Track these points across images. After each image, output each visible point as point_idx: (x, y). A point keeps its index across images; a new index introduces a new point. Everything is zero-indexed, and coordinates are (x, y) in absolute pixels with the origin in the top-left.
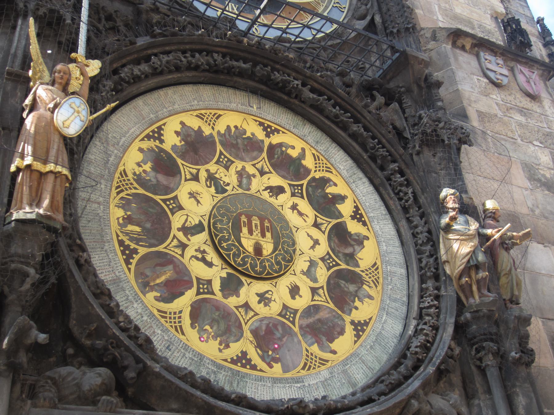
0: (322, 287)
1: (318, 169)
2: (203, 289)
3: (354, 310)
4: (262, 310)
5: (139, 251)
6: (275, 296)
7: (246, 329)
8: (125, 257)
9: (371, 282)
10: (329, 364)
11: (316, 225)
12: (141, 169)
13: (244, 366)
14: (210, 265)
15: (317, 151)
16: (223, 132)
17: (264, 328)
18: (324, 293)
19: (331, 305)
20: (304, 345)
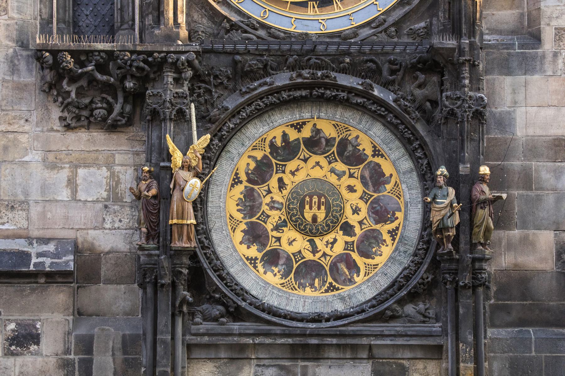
0: (349, 169)
4: (364, 213)
6: (354, 202)
7: (374, 227)
9: (347, 133)
10: (398, 181)
11: (305, 160)
12: (278, 274)
13: (396, 234)
14: (335, 240)
16: (242, 215)
17: (374, 216)
19: (361, 166)
20: (385, 193)
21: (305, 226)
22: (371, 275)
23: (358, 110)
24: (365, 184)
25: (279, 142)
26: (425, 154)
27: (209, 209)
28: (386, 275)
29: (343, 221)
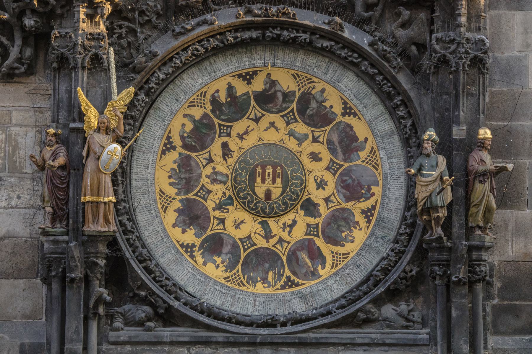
0: (313, 132)
1: (203, 105)
2: (314, 231)
3: (332, 110)
5: (288, 275)
6: (319, 174)
7: (344, 205)
8: (294, 286)
10: (375, 147)
11: (257, 120)
12: (221, 265)
13: (372, 215)
14: (295, 222)
15: (186, 102)
16: (176, 191)
17: (344, 191)
18: (317, 132)
19: (328, 128)
20: (358, 162)
21: (255, 204)
22: (339, 267)
23: (324, 56)
24: (332, 150)
25: (223, 97)
26: (409, 112)
27: (134, 182)
28: (359, 266)
29: (305, 198)
